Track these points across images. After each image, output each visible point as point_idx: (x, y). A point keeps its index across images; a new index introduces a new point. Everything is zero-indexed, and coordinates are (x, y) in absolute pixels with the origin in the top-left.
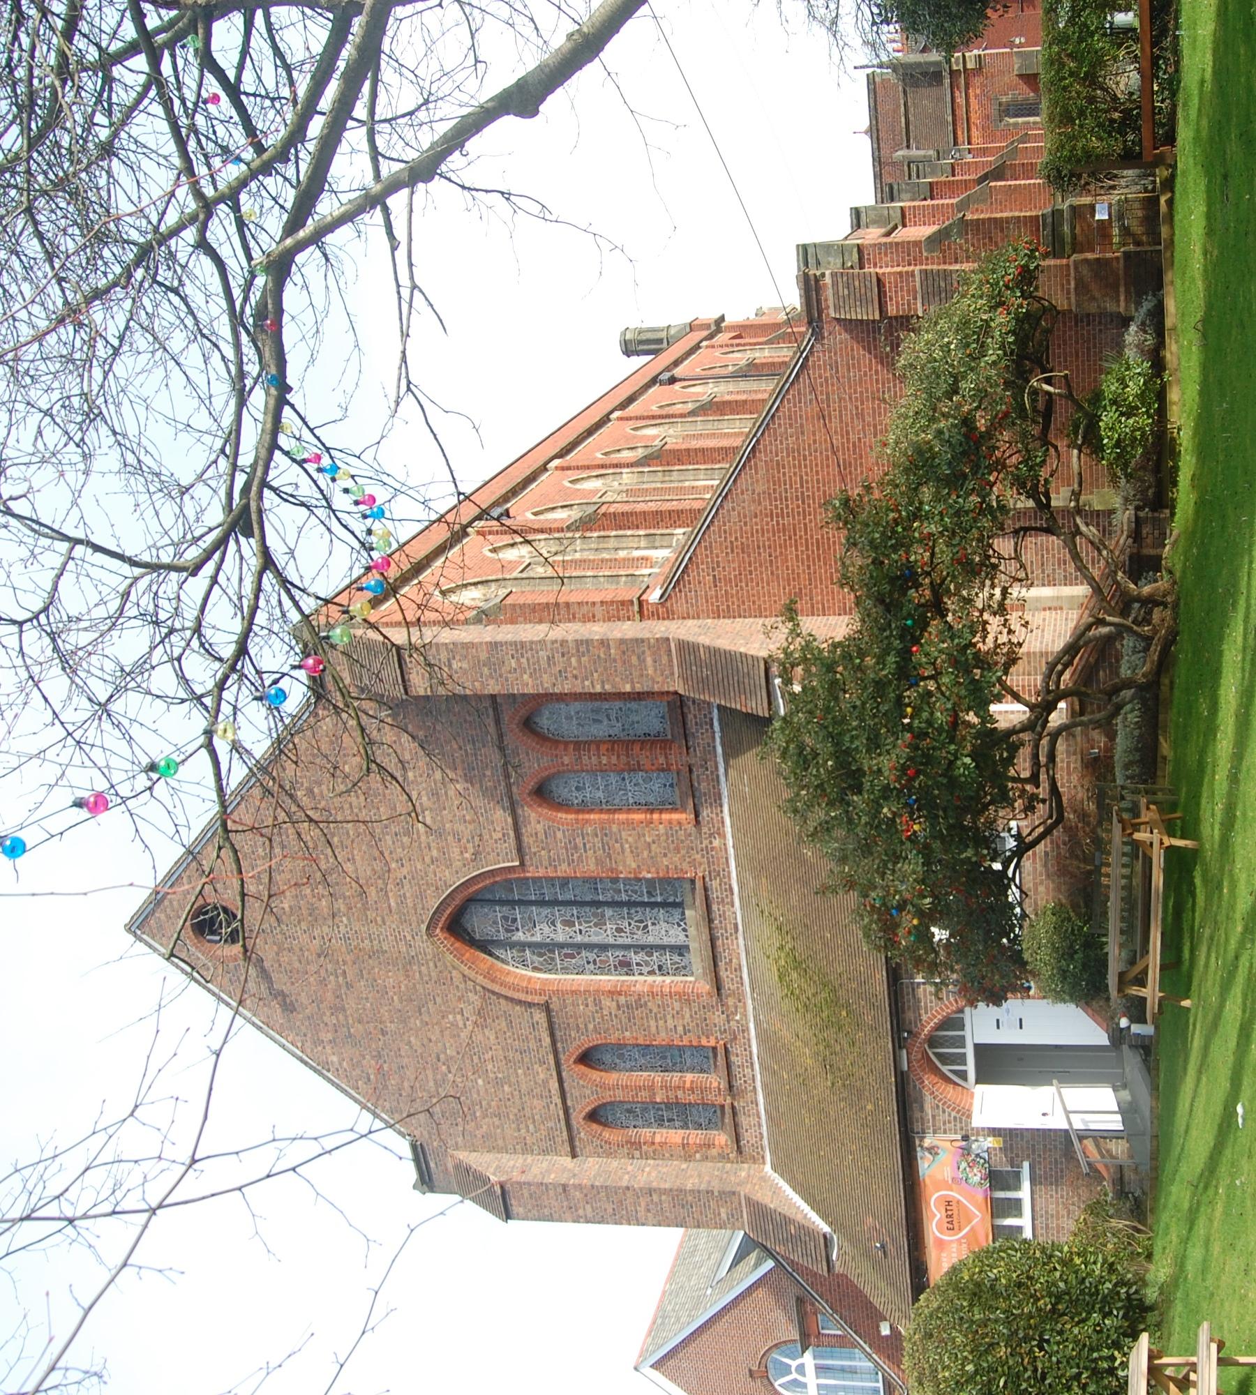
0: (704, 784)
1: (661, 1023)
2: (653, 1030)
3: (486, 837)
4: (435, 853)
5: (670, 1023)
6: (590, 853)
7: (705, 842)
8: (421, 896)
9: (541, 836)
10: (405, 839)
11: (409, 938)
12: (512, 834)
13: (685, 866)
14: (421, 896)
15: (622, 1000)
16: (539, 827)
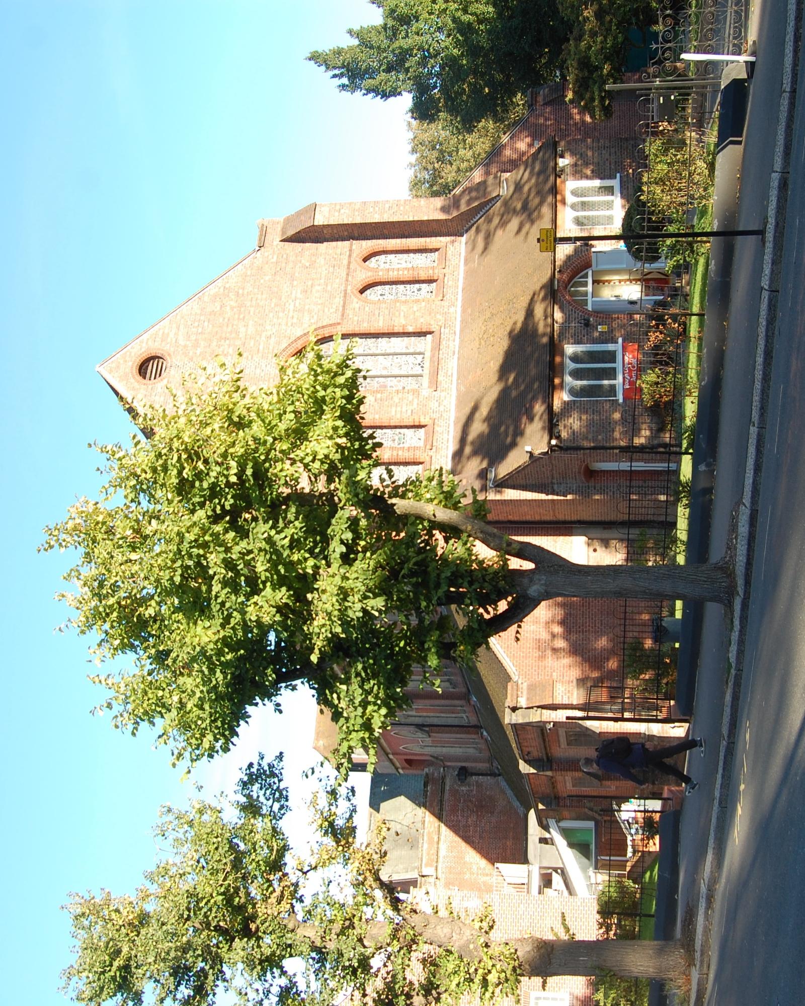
0: (450, 283)
1: (399, 409)
2: (393, 413)
3: (326, 310)
4: (295, 320)
5: (404, 410)
6: (381, 318)
7: (446, 310)
8: (279, 343)
9: (357, 310)
10: (281, 314)
11: (264, 366)
12: (341, 309)
13: (432, 322)
14: (279, 343)
15: (379, 396)
16: (357, 306)
